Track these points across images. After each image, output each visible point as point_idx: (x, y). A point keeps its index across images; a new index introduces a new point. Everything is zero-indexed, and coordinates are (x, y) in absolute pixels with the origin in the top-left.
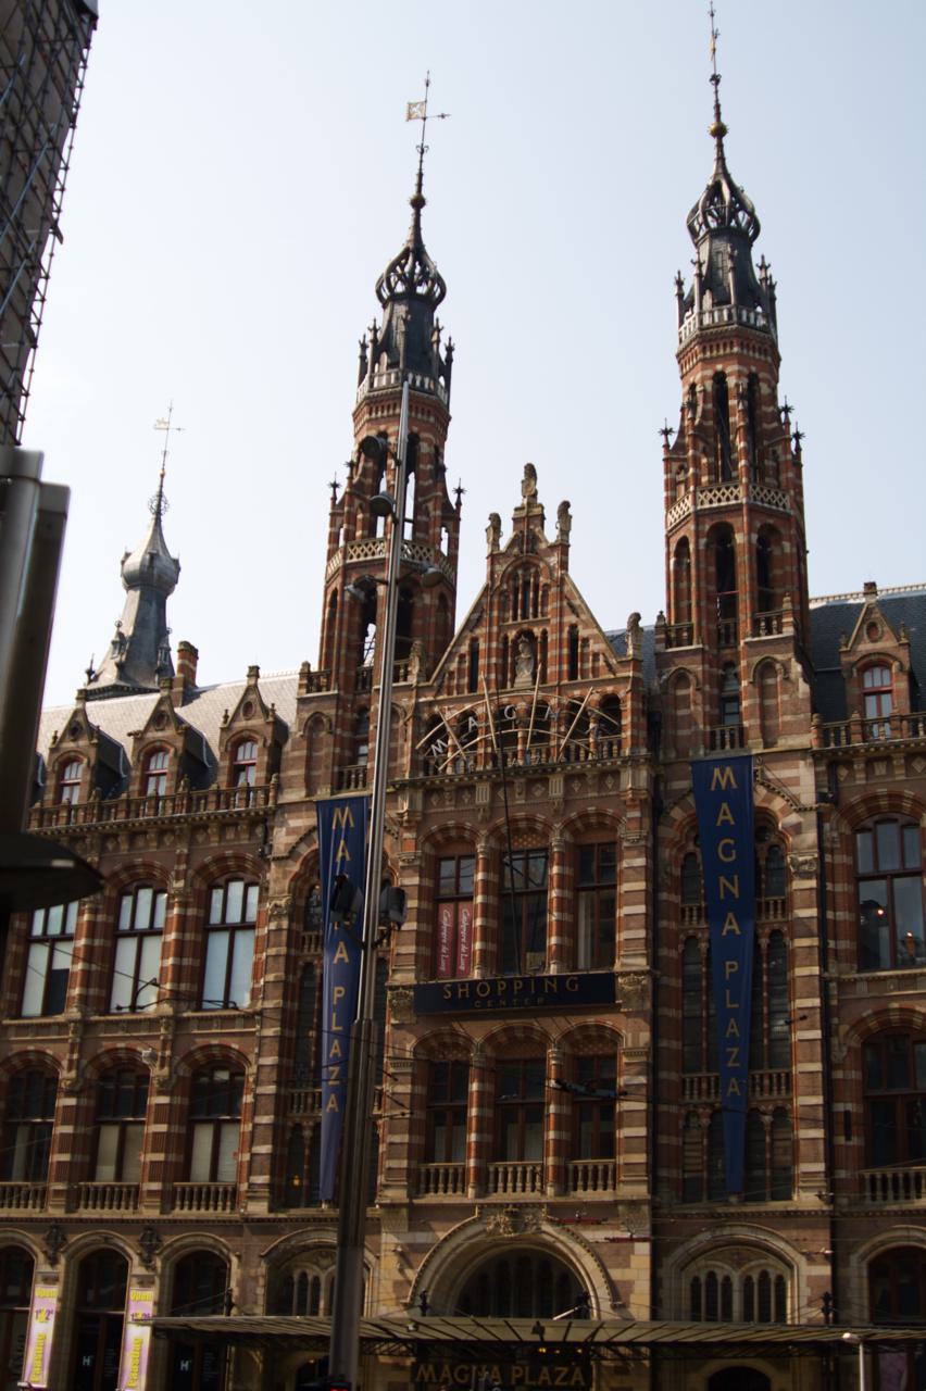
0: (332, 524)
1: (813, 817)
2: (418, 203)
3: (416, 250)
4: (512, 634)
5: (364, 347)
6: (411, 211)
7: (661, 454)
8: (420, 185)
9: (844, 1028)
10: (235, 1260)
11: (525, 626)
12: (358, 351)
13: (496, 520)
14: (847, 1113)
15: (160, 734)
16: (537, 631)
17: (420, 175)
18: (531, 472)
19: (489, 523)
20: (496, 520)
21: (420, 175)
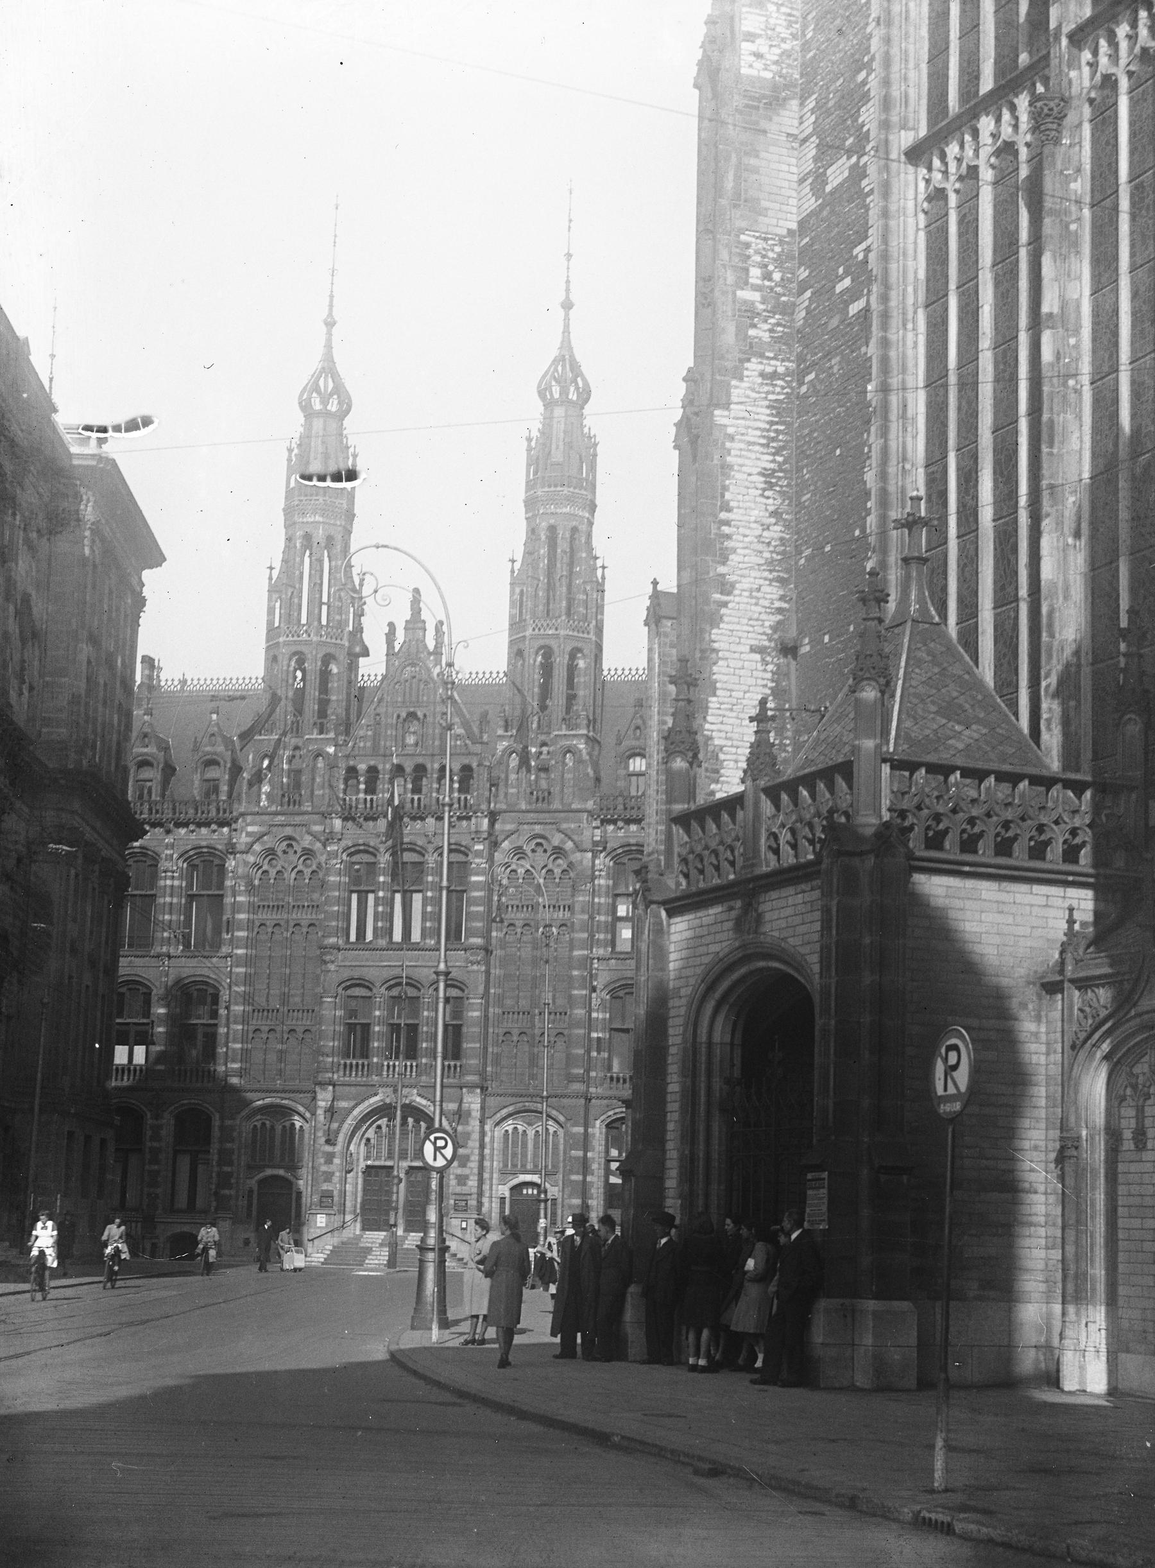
0: (270, 600)
1: (590, 855)
2: (330, 324)
3: (329, 368)
4: (404, 715)
5: (290, 450)
6: (324, 329)
7: (507, 579)
8: (331, 306)
9: (600, 987)
10: (217, 1116)
11: (412, 710)
12: (286, 454)
13: (391, 625)
14: (599, 1038)
15: (145, 750)
16: (420, 714)
17: (332, 297)
18: (417, 591)
19: (387, 630)
20: (391, 625)
21: (332, 297)
